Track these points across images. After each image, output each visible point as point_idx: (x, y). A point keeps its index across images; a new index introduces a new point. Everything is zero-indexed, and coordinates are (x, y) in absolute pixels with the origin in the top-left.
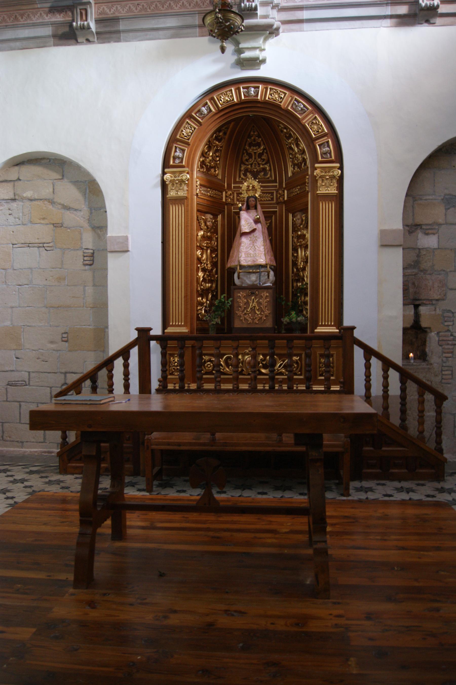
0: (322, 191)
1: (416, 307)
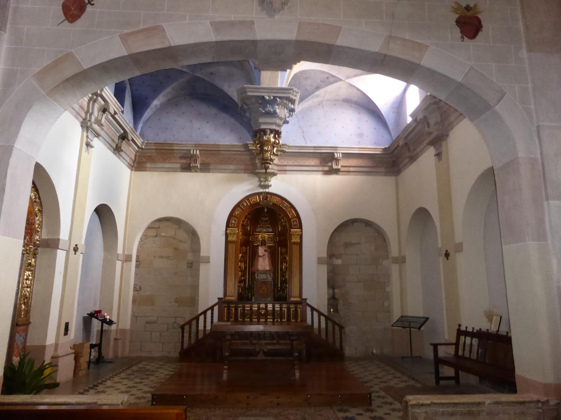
0: (294, 240)
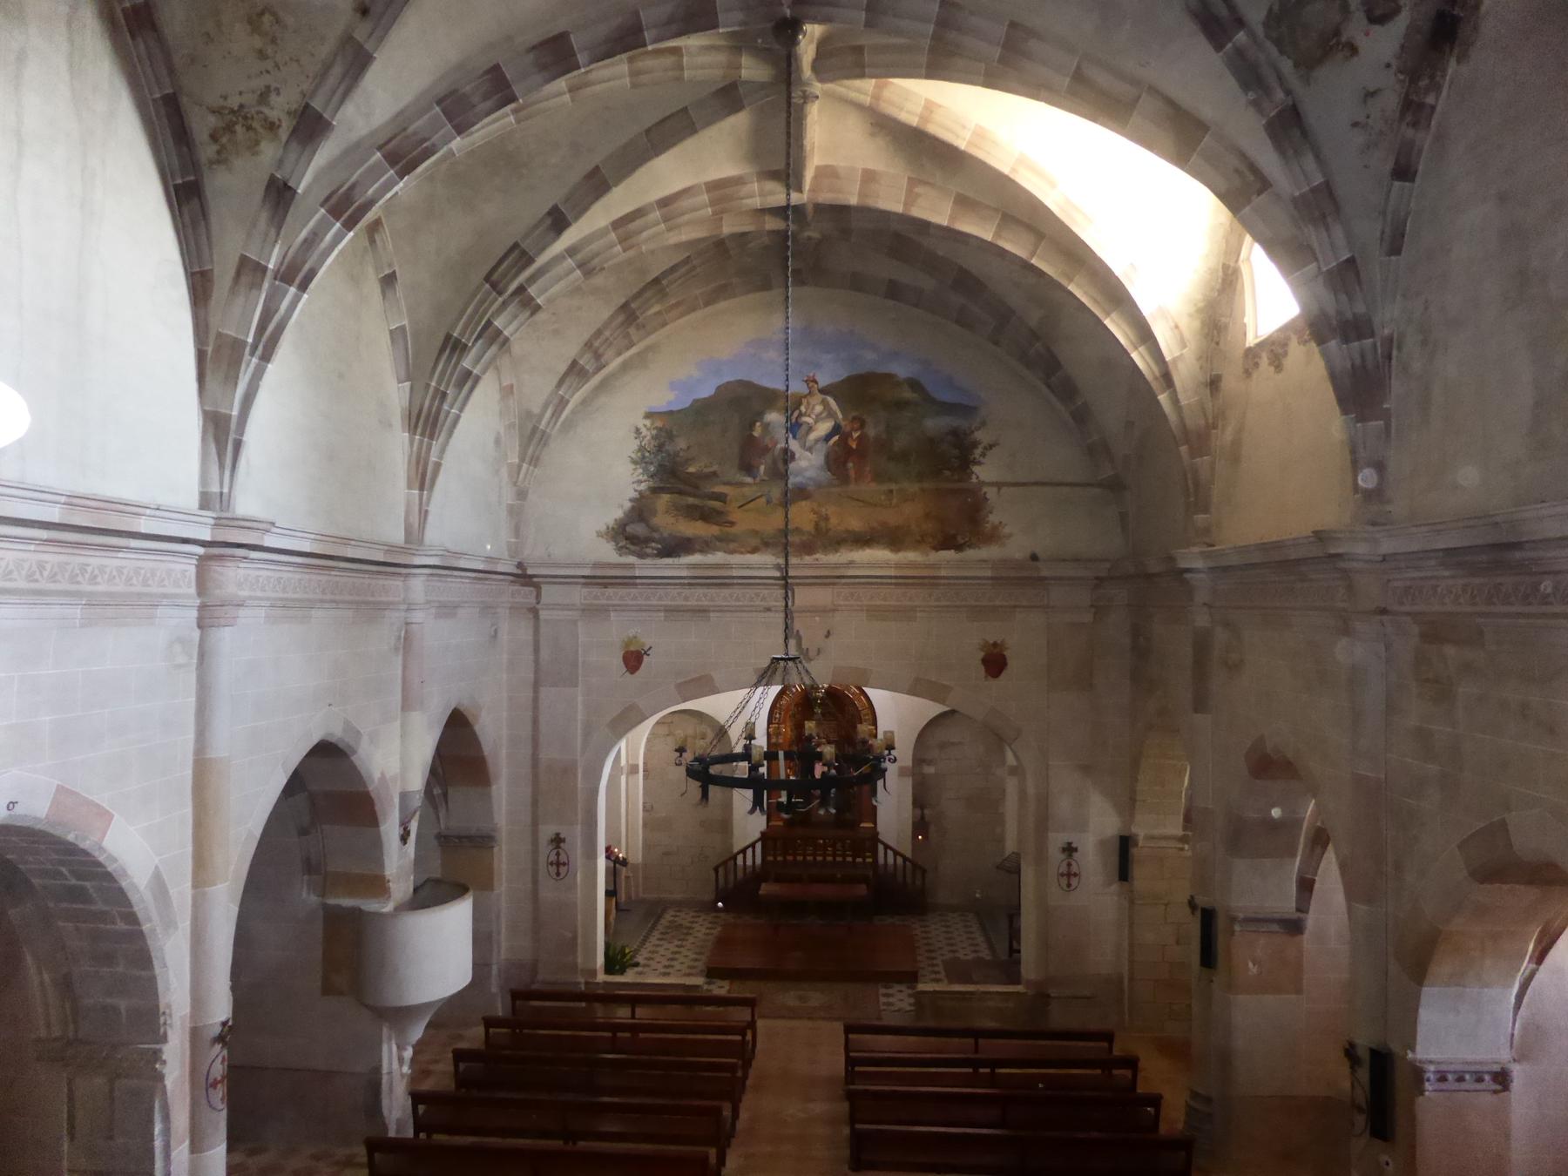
1: (922, 808)
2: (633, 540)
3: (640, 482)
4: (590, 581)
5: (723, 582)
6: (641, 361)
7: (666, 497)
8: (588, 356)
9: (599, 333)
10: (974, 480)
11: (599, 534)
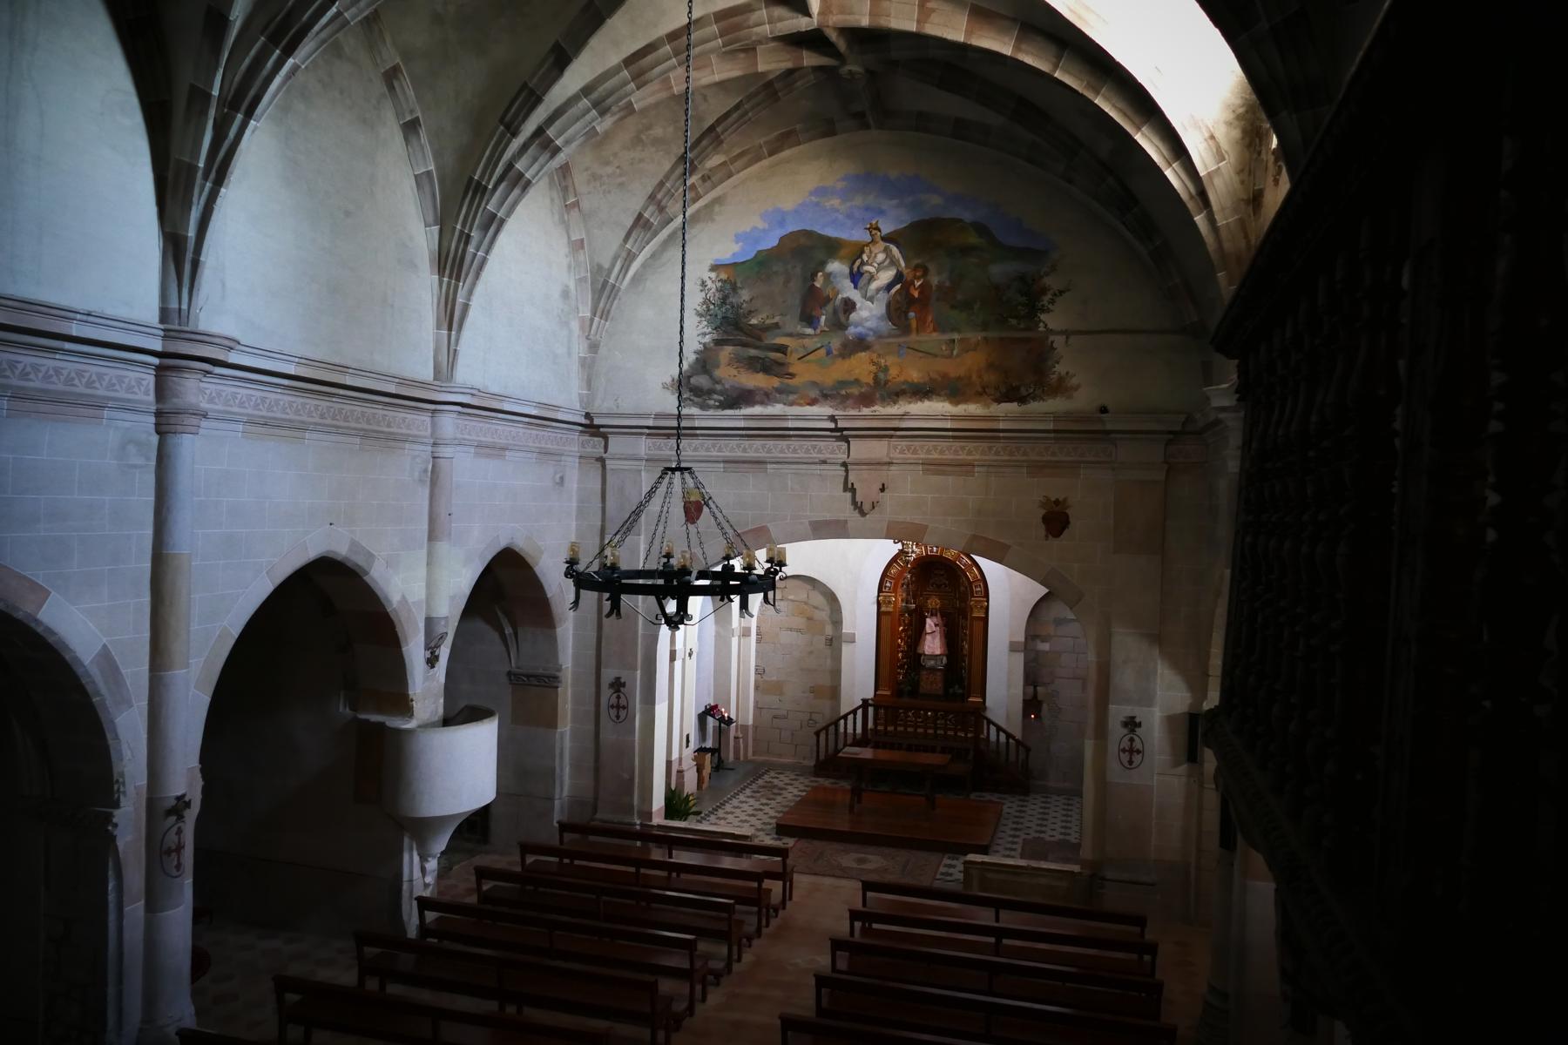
2: (697, 391)
3: (704, 334)
4: (655, 431)
5: (781, 434)
6: (707, 214)
7: (729, 349)
8: (651, 208)
9: (661, 184)
10: (1042, 329)
11: (665, 387)
